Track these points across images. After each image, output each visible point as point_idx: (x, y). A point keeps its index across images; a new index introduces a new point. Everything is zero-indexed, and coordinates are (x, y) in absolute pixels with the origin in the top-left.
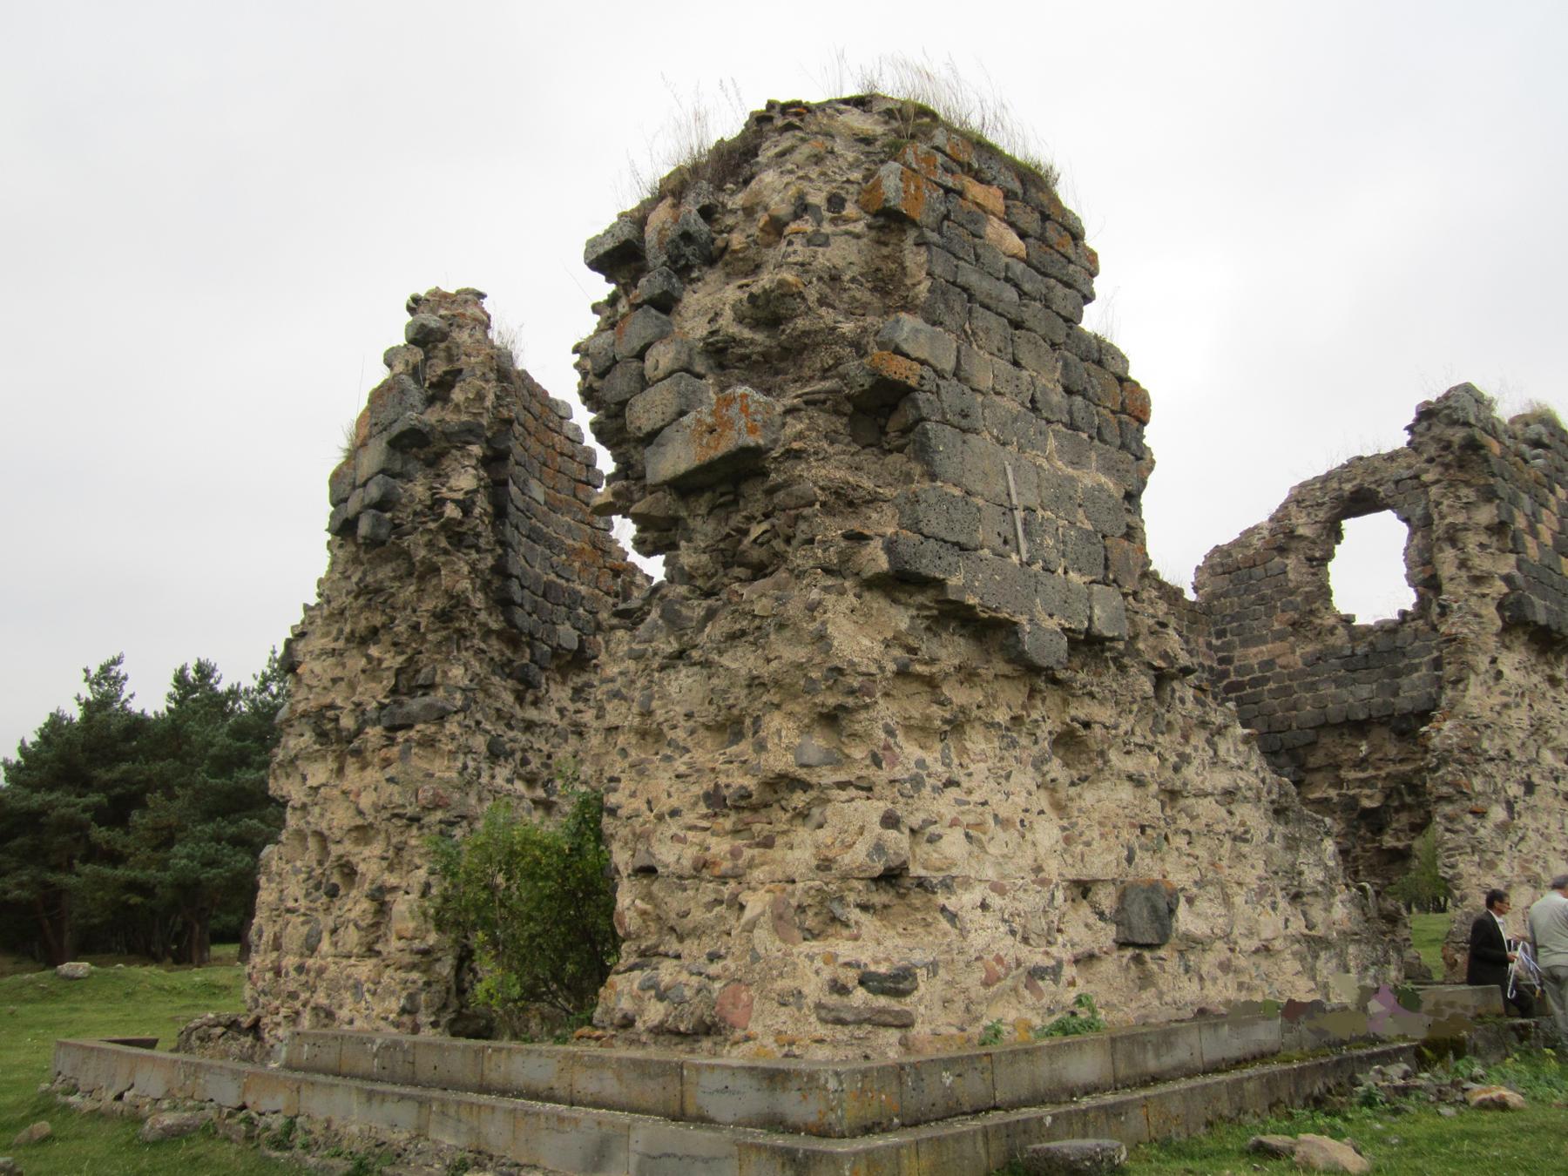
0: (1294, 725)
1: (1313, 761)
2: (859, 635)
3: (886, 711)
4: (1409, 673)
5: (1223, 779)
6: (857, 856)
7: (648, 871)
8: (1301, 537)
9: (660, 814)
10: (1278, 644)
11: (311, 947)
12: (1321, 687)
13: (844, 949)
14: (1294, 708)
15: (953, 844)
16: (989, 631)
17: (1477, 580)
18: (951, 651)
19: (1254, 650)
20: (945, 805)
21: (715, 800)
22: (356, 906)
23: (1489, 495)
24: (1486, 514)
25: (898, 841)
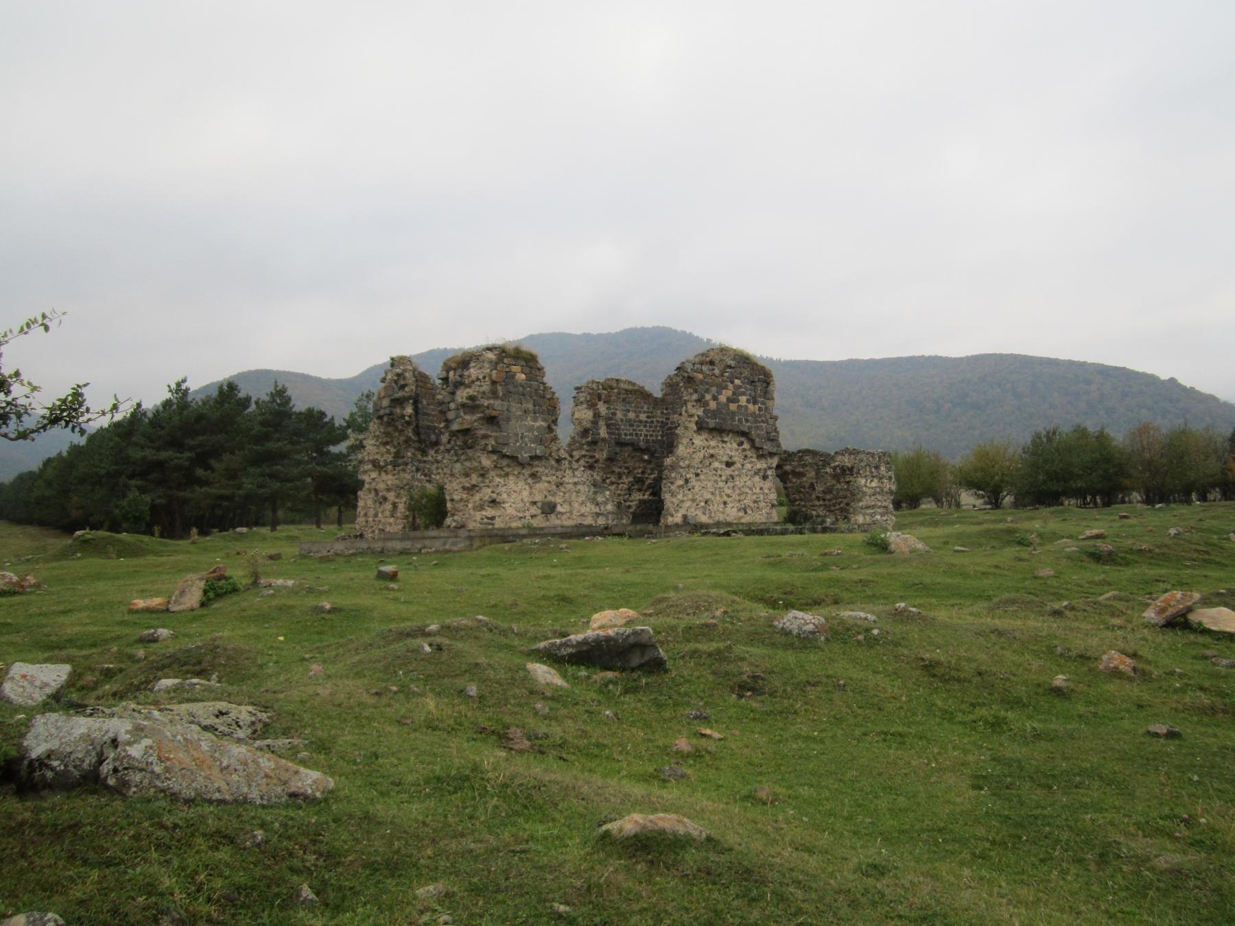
2: (486, 462)
3: (492, 473)
5: (576, 480)
6: (487, 498)
7: (452, 500)
9: (454, 490)
11: (376, 515)
13: (484, 513)
15: (505, 496)
16: (513, 458)
17: (691, 416)
18: (505, 462)
20: (503, 489)
21: (464, 488)
22: (388, 506)
23: (696, 391)
24: (695, 397)
25: (494, 496)
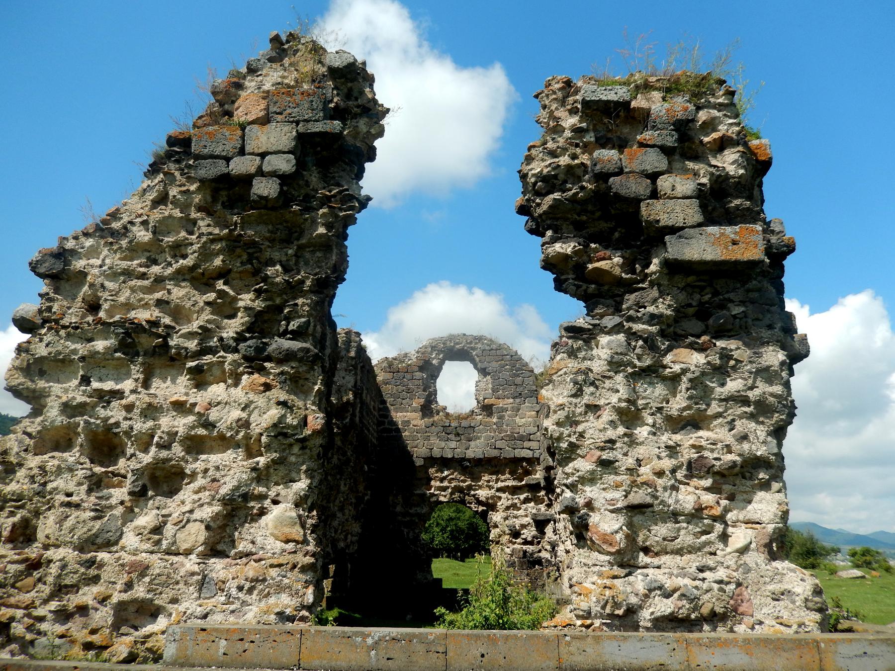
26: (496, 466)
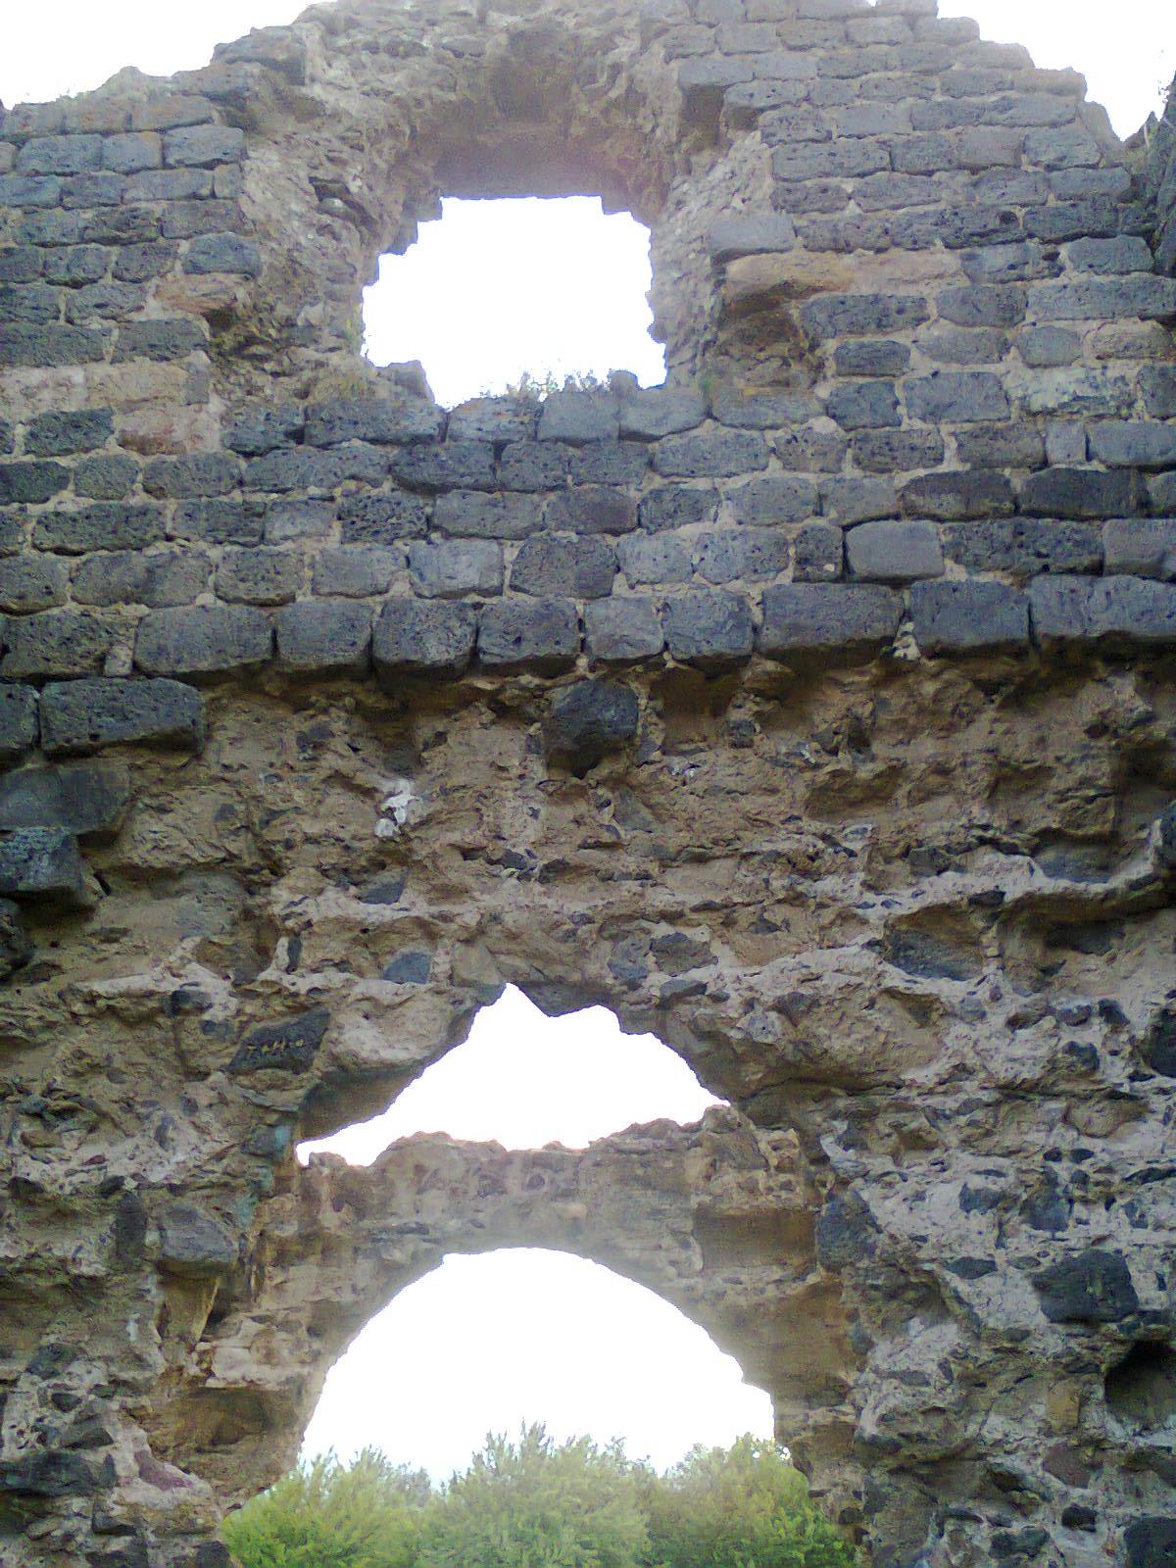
0: (121, 660)
1: (151, 837)
4: (672, 518)
8: (312, 112)
10: (144, 363)
12: (278, 527)
14: (142, 592)
19: (36, 376)
26: (859, 741)
